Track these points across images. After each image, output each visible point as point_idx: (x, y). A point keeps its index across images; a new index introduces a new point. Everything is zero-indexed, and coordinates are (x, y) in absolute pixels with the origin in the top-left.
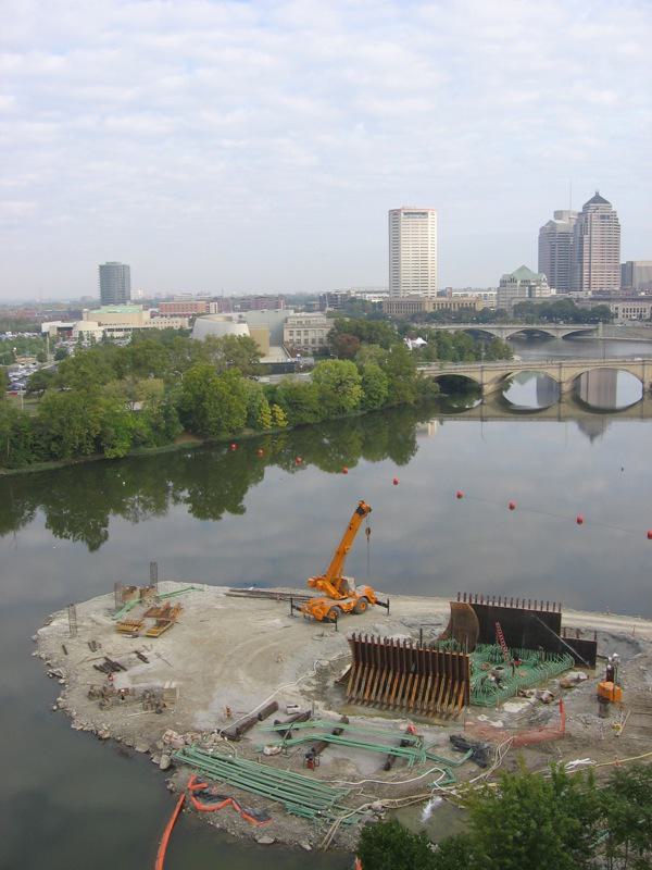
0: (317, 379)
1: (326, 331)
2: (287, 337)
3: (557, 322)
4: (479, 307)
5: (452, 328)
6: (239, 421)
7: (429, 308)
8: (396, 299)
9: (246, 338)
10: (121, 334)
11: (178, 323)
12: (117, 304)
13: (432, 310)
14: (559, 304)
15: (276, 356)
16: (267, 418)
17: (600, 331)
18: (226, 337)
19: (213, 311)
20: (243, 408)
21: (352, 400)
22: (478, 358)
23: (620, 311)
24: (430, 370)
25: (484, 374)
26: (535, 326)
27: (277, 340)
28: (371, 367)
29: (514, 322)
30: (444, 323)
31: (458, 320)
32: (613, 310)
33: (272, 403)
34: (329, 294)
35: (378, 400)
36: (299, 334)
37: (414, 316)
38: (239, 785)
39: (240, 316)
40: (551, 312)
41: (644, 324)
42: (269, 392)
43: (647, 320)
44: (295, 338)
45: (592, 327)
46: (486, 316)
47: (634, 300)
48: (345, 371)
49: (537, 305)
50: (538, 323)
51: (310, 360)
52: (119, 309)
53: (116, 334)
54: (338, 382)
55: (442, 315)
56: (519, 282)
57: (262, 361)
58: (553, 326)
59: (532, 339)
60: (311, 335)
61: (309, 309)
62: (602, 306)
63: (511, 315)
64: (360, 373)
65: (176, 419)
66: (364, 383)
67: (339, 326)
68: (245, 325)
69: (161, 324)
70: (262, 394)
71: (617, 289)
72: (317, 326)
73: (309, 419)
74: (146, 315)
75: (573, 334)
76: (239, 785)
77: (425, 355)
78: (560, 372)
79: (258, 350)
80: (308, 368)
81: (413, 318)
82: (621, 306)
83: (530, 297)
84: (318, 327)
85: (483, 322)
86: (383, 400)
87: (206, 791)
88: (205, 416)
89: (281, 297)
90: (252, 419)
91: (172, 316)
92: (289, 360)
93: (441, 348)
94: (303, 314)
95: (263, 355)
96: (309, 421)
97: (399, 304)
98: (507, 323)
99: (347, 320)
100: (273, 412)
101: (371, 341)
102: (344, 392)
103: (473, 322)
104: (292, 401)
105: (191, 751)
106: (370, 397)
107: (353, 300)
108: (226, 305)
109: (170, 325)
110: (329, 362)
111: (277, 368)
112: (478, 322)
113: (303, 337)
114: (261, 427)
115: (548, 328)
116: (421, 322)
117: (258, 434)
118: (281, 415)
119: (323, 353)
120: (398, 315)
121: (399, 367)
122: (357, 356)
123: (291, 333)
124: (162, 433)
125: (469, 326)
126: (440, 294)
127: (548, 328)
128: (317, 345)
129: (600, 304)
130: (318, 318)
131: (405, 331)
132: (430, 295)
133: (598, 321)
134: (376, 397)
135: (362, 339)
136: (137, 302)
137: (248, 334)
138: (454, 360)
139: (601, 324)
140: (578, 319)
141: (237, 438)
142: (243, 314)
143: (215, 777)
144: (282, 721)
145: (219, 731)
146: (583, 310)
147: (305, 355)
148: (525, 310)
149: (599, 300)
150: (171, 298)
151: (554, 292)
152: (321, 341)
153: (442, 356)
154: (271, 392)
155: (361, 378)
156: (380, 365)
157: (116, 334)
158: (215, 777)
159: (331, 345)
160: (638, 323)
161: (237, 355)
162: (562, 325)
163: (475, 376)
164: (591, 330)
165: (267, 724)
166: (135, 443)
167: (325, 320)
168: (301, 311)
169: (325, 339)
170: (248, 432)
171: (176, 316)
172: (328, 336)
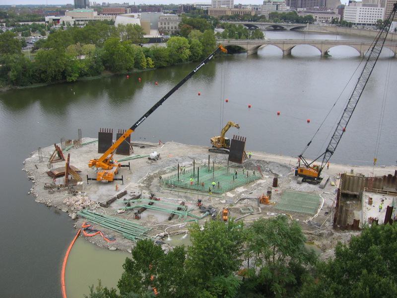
0: (169, 46)
1: (178, 23)
2: (159, 26)
3: (288, 22)
4: (253, 14)
5: (237, 23)
6: (131, 64)
7: (229, 14)
8: (215, 9)
9: (138, 26)
10: (83, 23)
11: (109, 18)
12: (81, 8)
13: (231, 14)
14: (290, 14)
15: (154, 34)
16: (144, 64)
17: (307, 27)
18: (128, 24)
19: (128, 11)
20: (132, 59)
21: (185, 56)
22: (247, 37)
23: (318, 19)
24: (223, 43)
25: (248, 45)
26: (278, 24)
27: (155, 27)
28: (195, 41)
29: (268, 21)
30: (235, 21)
31: (242, 20)
32: (314, 18)
33: (147, 57)
34: (183, 5)
35: (198, 57)
36: (165, 24)
37: (223, 17)
38: (105, 226)
39: (139, 15)
40: (285, 17)
41: (328, 25)
42: (146, 52)
43: (329, 23)
44: (163, 26)
45: (304, 25)
46: (255, 18)
47: (325, 13)
48: (182, 42)
49: (280, 14)
50: (279, 22)
51: (169, 37)
52: (82, 10)
53: (80, 23)
54: (179, 47)
55: (235, 17)
56: (272, 3)
57: (145, 36)
58: (286, 24)
59: (276, 28)
60: (171, 25)
61: (174, 13)
62: (309, 16)
63: (267, 18)
64: (189, 43)
65: (101, 63)
66: (191, 48)
67: (184, 21)
68: (139, 20)
69: (102, 18)
70: (142, 52)
71: (318, 8)
72: (177, 21)
73: (165, 64)
74: (95, 14)
75: (293, 28)
76: (105, 226)
77: (224, 36)
78: (283, 46)
79: (144, 31)
80: (166, 41)
81: (221, 18)
82: (318, 15)
83: (277, 9)
84: (174, 22)
85: (254, 21)
86: (200, 57)
87: (89, 228)
88: (114, 62)
89: (162, 6)
90: (137, 64)
91: (108, 15)
92: (159, 37)
93: (232, 33)
94: (168, 15)
95: (145, 34)
96: (165, 65)
97: (216, 11)
98: (265, 22)
99: (188, 18)
100: (147, 61)
101: (198, 28)
102: (182, 52)
103: (249, 21)
104: (157, 56)
105: (85, 211)
106: (194, 55)
107: (195, 9)
108: (134, 9)
109: (107, 19)
110: (175, 38)
111: (152, 40)
112: (251, 21)
113: (167, 26)
114: (142, 68)
115: (283, 24)
116: (225, 20)
117: (140, 71)
118: (151, 62)
119: (176, 33)
120: (215, 17)
121: (208, 43)
122: (189, 36)
123: (161, 24)
124: (93, 70)
125: (247, 23)
126: (236, 7)
127: (283, 24)
128: (174, 29)
129: (308, 14)
130: (175, 17)
131: (216, 24)
132: (230, 7)
133: (306, 23)
134: (196, 55)
135: (194, 27)
136: (92, 7)
137: (140, 25)
138: (236, 39)
139: (308, 24)
140: (298, 22)
141: (130, 73)
142: (140, 14)
143: (94, 222)
144: (127, 199)
145: (99, 203)
146: (301, 17)
147: (167, 34)
148: (273, 16)
149: (308, 12)
150: (109, 5)
151: (288, 8)
152: (175, 28)
153: (231, 36)
154: (147, 53)
155: (189, 46)
156: (200, 40)
157: (80, 23)
158: (94, 222)
159: (180, 30)
160: (326, 24)
161: (133, 34)
162: (290, 24)
163: (244, 46)
164: (303, 27)
165: (121, 200)
166: (81, 75)
167: (178, 18)
168: (167, 13)
169: (177, 27)
170: (135, 70)
171: (110, 14)
172: (179, 26)
